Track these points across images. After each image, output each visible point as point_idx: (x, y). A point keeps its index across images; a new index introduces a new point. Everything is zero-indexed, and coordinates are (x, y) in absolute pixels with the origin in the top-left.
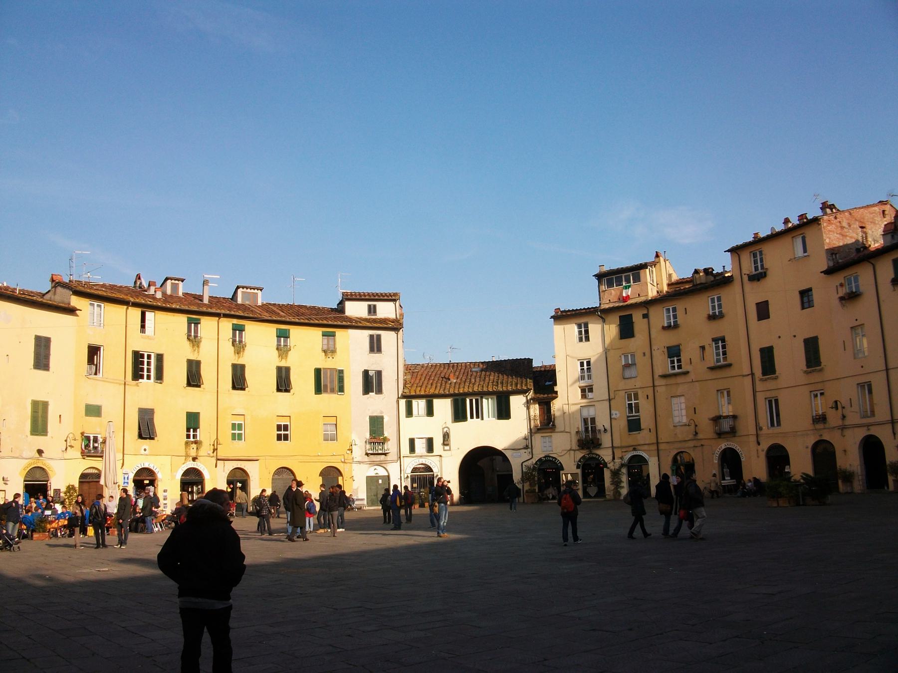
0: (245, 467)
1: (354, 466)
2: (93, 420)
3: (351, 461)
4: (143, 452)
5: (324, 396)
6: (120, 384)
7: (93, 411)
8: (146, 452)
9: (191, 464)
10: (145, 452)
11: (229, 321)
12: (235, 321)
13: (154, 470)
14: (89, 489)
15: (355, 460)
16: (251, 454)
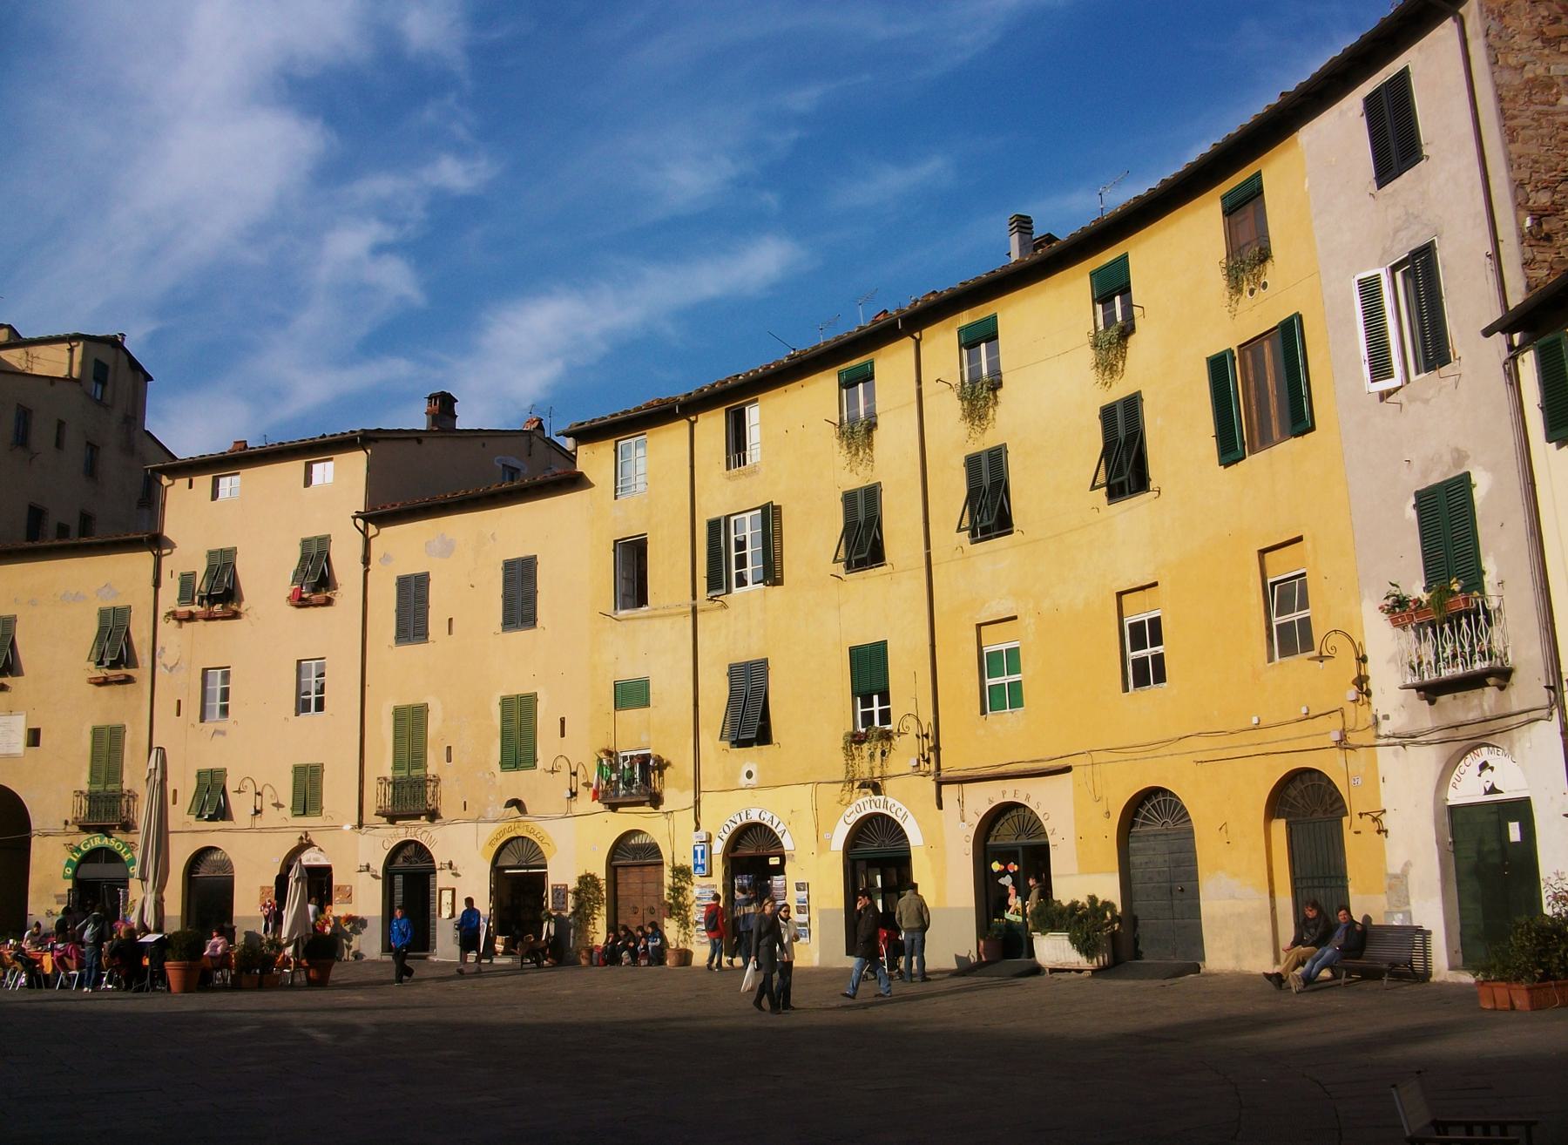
0: (1028, 798)
1: (1386, 758)
2: (631, 716)
3: (1367, 738)
4: (744, 780)
5: (1255, 463)
6: (684, 614)
7: (631, 694)
8: (753, 781)
9: (866, 804)
10: (749, 781)
11: (948, 329)
12: (965, 318)
13: (773, 827)
14: (643, 883)
15: (1385, 729)
16: (1045, 751)
